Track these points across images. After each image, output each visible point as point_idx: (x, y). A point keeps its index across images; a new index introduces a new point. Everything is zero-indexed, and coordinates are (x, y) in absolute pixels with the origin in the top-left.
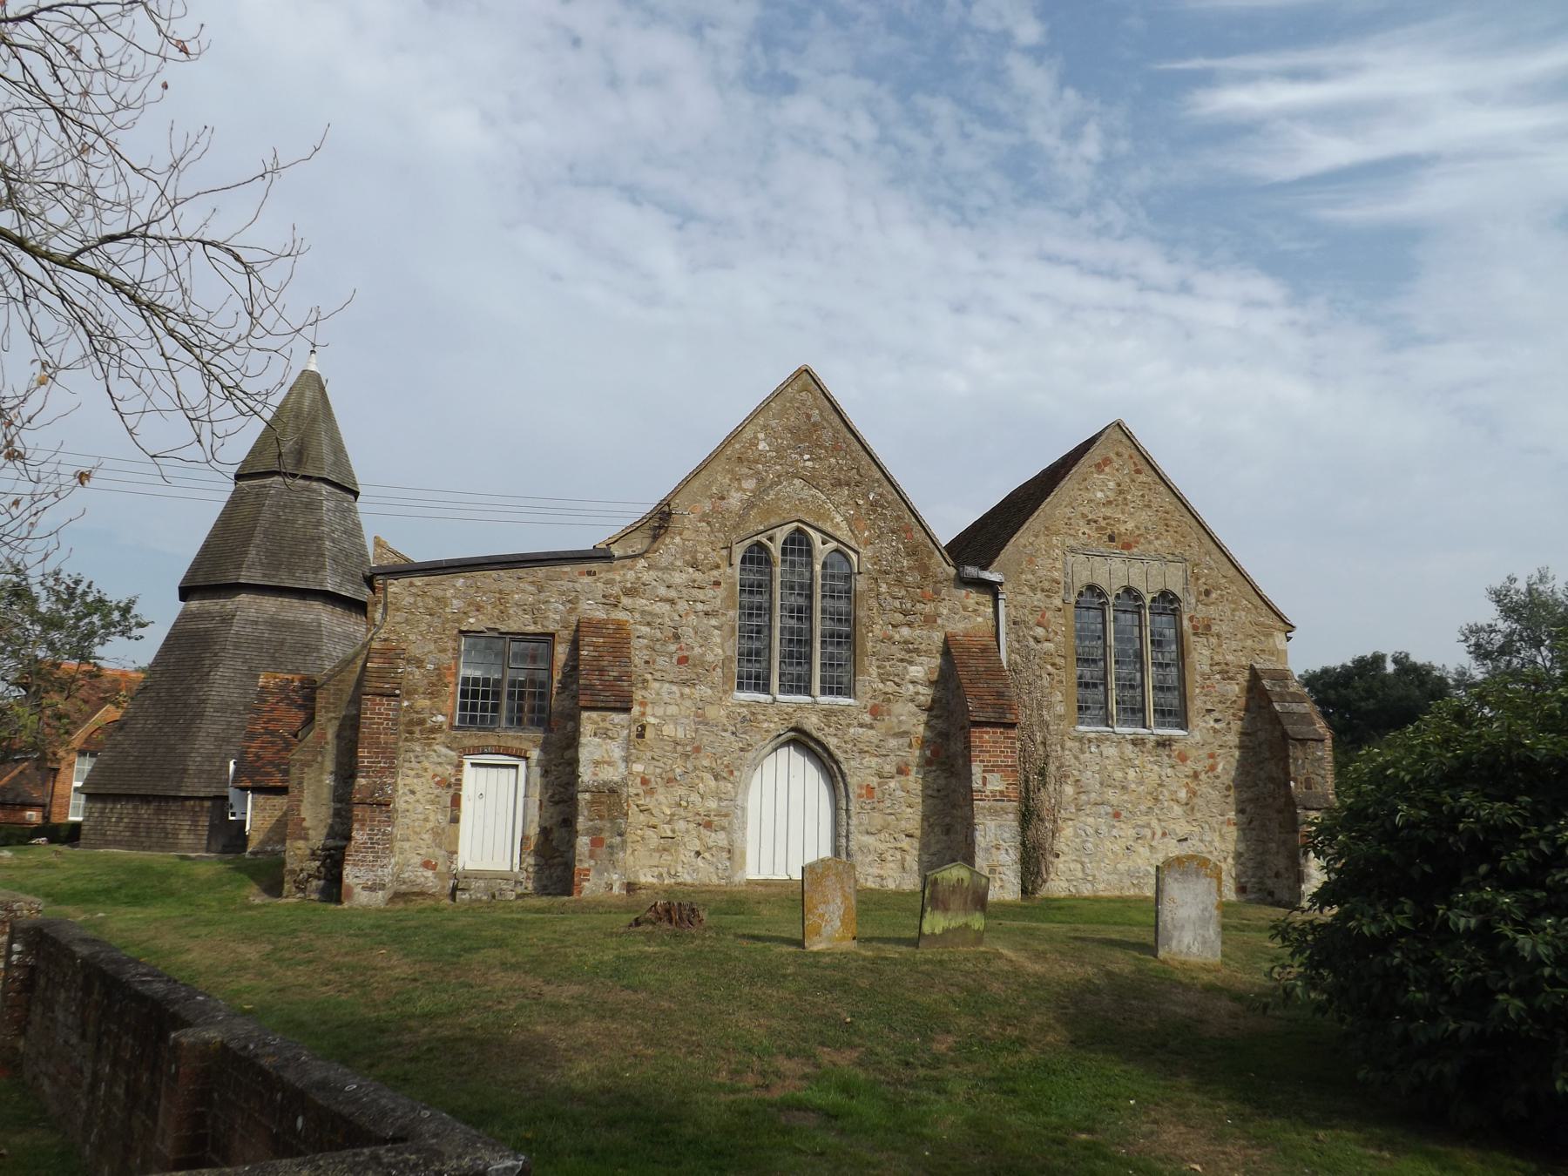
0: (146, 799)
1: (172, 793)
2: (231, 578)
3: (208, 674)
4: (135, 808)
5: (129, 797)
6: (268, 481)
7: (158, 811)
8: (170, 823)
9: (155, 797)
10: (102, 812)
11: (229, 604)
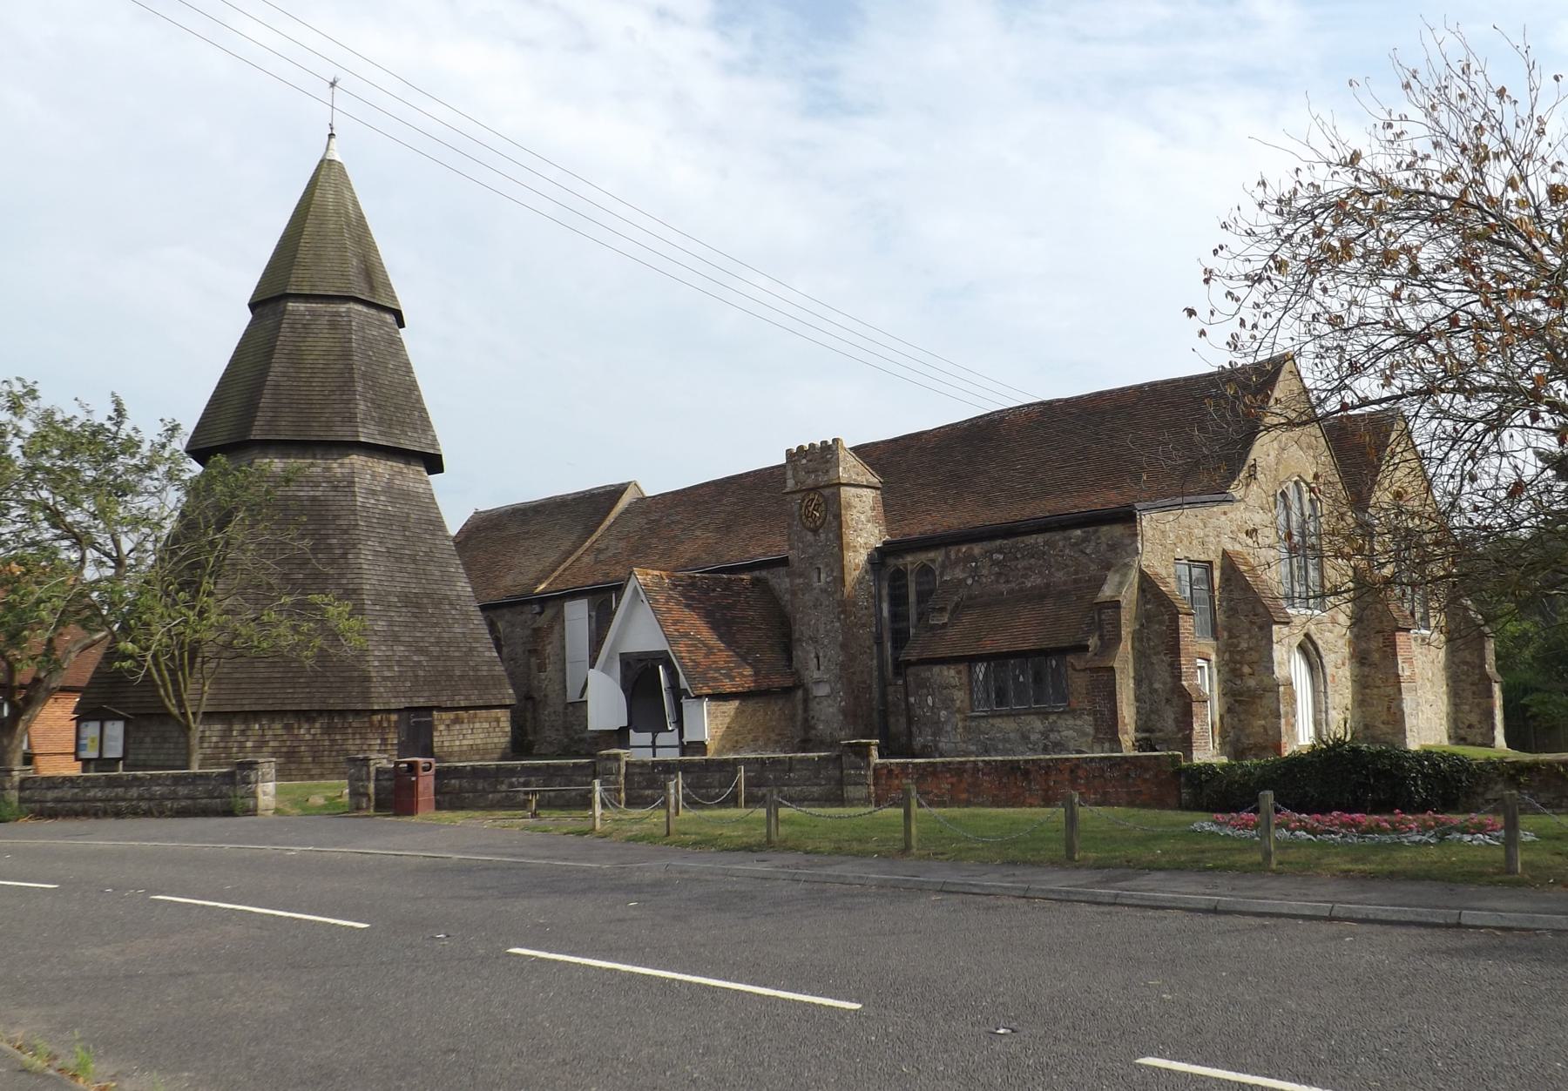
0: (307, 716)
1: (360, 707)
2: (342, 433)
3: (344, 555)
4: (288, 727)
5: (273, 714)
6: (343, 308)
7: (328, 730)
8: (352, 745)
9: (320, 712)
10: (226, 736)
11: (339, 466)
